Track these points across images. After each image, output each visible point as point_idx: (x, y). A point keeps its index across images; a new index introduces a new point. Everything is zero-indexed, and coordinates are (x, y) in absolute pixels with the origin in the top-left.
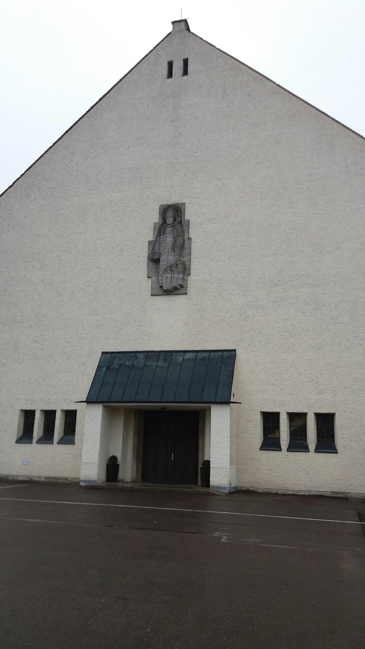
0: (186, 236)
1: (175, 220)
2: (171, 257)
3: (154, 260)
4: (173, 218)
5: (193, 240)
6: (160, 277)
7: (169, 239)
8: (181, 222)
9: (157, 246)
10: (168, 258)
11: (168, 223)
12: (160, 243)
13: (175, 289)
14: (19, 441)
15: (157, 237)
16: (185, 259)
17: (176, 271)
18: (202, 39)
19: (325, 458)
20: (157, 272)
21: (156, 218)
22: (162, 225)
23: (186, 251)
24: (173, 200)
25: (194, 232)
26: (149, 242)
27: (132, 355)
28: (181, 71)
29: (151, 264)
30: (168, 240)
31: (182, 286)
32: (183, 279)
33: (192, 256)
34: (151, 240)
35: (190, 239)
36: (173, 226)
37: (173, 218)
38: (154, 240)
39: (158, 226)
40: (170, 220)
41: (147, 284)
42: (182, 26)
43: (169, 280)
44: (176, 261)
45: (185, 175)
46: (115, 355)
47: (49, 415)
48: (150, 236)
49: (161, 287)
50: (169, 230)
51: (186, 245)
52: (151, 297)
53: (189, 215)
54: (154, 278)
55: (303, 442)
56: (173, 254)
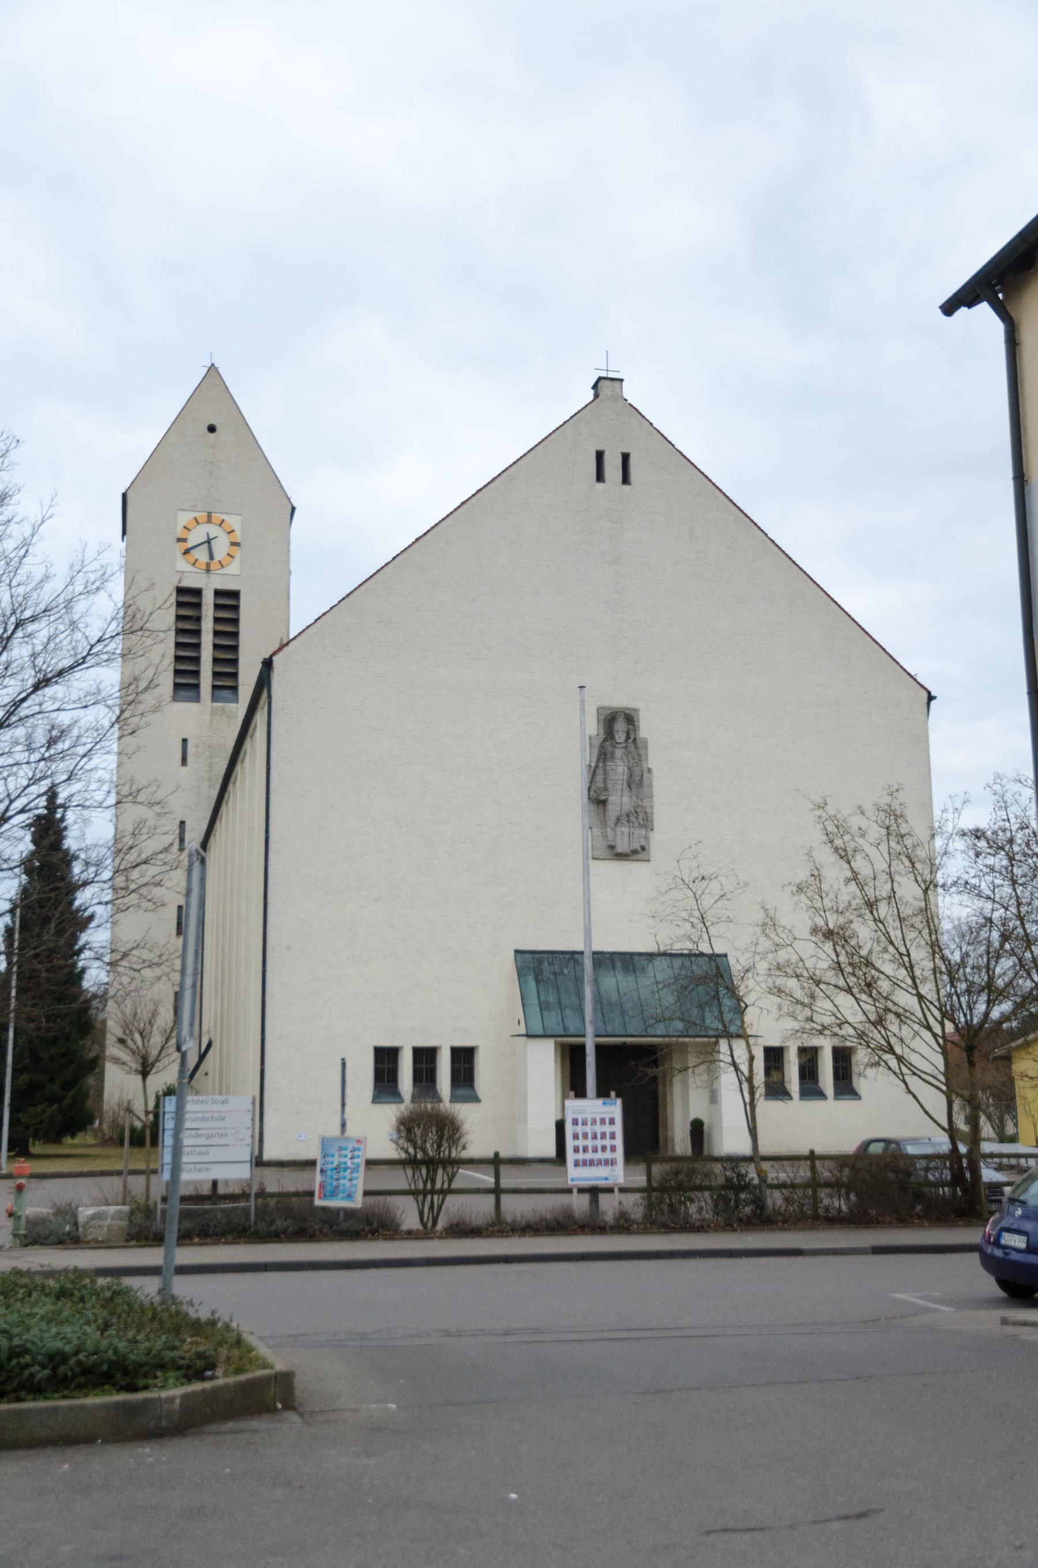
0: (645, 766)
1: (628, 737)
2: (625, 799)
3: (598, 801)
4: (618, 729)
5: (655, 772)
6: (609, 829)
7: (619, 769)
8: (635, 739)
9: (599, 778)
10: (619, 801)
13: (635, 852)
14: (377, 1099)
15: (598, 761)
16: (645, 803)
17: (637, 825)
18: (651, 424)
19: (846, 1106)
20: (603, 822)
21: (593, 727)
22: (605, 740)
24: (619, 701)
25: (655, 759)
27: (567, 956)
28: (607, 457)
29: (593, 807)
30: (620, 769)
31: (643, 848)
32: (647, 838)
33: (655, 799)
35: (649, 770)
36: (626, 748)
37: (618, 729)
38: (593, 765)
39: (597, 743)
40: (620, 737)
43: (626, 838)
46: (538, 956)
47: (425, 1057)
49: (612, 847)
50: (619, 753)
51: (646, 782)
53: (646, 729)
55: (814, 1086)
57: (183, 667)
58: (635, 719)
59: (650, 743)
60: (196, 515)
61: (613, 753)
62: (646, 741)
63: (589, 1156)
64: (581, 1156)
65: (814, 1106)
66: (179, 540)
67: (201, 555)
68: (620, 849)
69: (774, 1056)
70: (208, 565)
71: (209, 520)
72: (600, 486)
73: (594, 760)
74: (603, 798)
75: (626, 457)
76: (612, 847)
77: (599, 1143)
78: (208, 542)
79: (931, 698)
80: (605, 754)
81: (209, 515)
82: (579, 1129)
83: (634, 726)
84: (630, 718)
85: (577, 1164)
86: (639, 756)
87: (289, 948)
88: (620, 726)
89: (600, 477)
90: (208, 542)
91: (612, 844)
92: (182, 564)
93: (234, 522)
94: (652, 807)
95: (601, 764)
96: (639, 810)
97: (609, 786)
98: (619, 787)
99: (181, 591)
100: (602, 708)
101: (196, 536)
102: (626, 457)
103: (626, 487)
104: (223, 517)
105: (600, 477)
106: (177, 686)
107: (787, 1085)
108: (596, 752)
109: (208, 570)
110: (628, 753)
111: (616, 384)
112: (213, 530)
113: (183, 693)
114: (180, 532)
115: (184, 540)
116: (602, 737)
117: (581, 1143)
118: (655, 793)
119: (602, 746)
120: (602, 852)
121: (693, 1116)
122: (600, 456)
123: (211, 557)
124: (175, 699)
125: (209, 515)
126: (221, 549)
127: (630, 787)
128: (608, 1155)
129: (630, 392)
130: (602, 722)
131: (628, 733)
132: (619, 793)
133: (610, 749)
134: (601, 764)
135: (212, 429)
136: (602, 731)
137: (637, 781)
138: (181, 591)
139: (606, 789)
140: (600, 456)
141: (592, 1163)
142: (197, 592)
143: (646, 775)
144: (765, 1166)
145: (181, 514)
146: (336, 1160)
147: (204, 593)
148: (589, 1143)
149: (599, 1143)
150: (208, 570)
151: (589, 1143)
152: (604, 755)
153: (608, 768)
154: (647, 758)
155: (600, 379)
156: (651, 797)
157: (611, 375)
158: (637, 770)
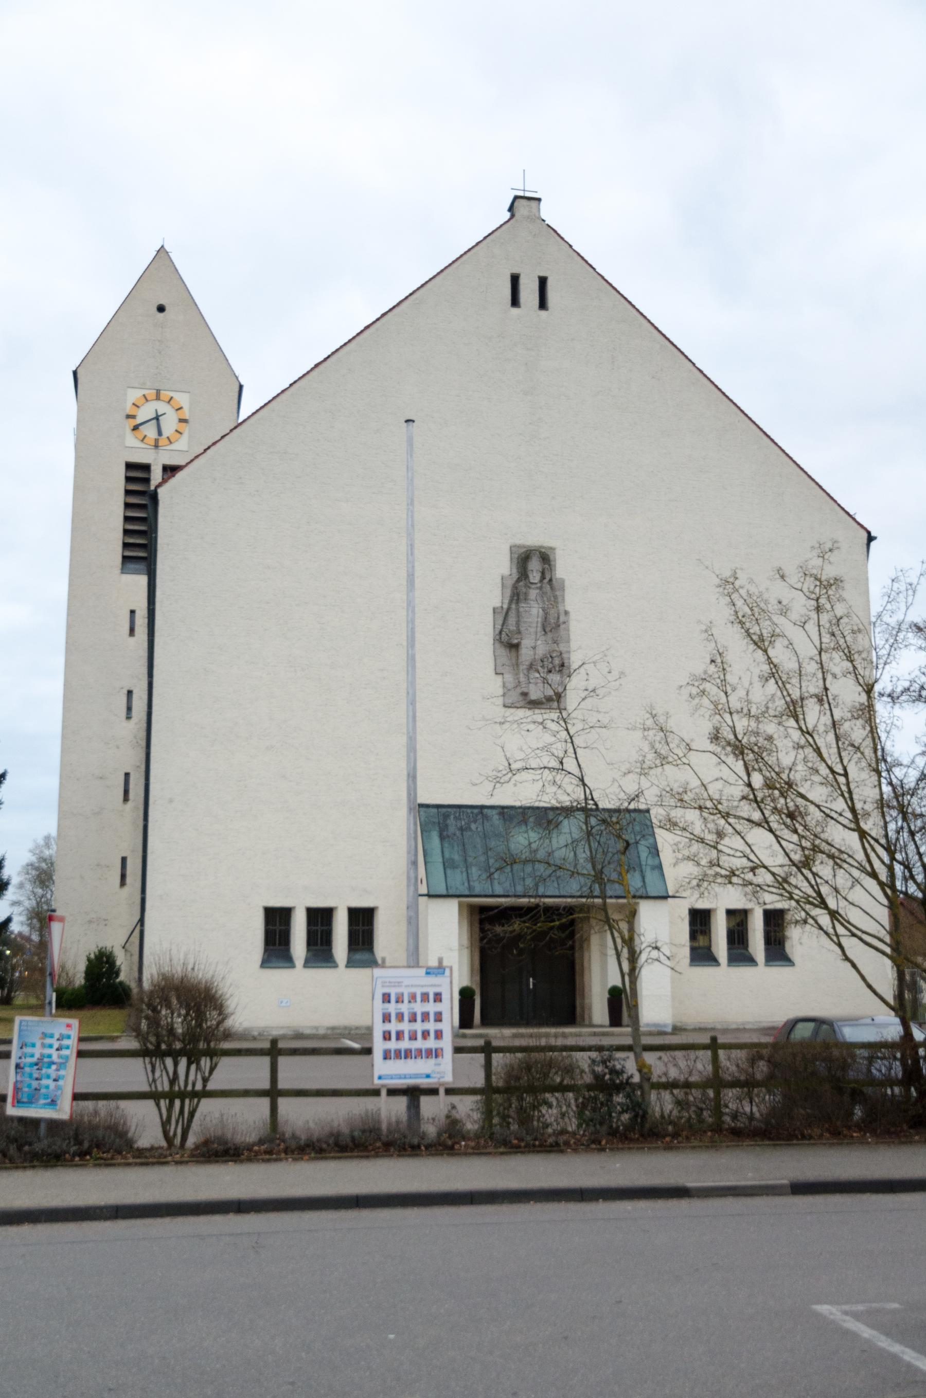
0: (561, 608)
3: (508, 643)
4: (532, 570)
5: (573, 616)
7: (533, 611)
8: (551, 580)
9: (512, 620)
10: (533, 645)
11: (532, 581)
12: (518, 615)
13: (549, 699)
14: (266, 963)
16: (562, 647)
18: (571, 246)
19: (778, 972)
20: (516, 665)
21: (504, 567)
22: (519, 580)
23: (562, 631)
24: (534, 539)
25: (572, 601)
26: (494, 609)
27: (476, 811)
29: (503, 652)
30: (534, 611)
34: (499, 605)
35: (566, 613)
36: (541, 588)
37: (532, 570)
38: (505, 606)
39: (510, 583)
40: (535, 577)
41: (495, 685)
42: (522, 205)
44: (550, 652)
45: (553, 498)
46: (444, 810)
47: (320, 919)
48: (496, 597)
49: (525, 694)
50: (533, 593)
52: (504, 709)
53: (562, 569)
54: (509, 677)
55: (743, 951)
56: (543, 638)
57: (131, 541)
58: (552, 558)
59: (567, 583)
60: (146, 392)
61: (526, 594)
62: (563, 581)
63: (405, 1044)
64: (393, 1045)
65: (744, 972)
66: (129, 417)
67: (150, 431)
68: (533, 696)
69: (700, 920)
70: (157, 441)
71: (158, 398)
72: (515, 311)
73: (507, 601)
74: (516, 641)
75: (543, 282)
76: (525, 694)
77: (419, 1027)
78: (157, 418)
79: (870, 538)
80: (518, 595)
81: (158, 392)
82: (392, 1008)
83: (550, 565)
84: (546, 558)
85: (387, 1055)
86: (556, 597)
87: (171, 801)
88: (535, 565)
89: (515, 302)
90: (157, 418)
91: (525, 690)
92: (131, 440)
93: (182, 399)
94: (569, 652)
95: (513, 606)
96: (554, 655)
97: (522, 629)
98: (532, 630)
99: (130, 466)
100: (515, 546)
101: (146, 412)
102: (543, 282)
103: (543, 313)
104: (171, 394)
105: (515, 302)
106: (125, 559)
107: (714, 949)
108: (508, 593)
109: (156, 446)
110: (543, 594)
111: (534, 204)
112: (162, 407)
113: (131, 566)
114: (129, 409)
115: (133, 417)
117: (393, 1027)
118: (572, 637)
120: (514, 696)
122: (515, 280)
123: (160, 433)
124: (124, 570)
125: (158, 392)
126: (169, 425)
127: (544, 631)
128: (431, 1043)
129: (547, 212)
130: (515, 561)
131: (543, 573)
132: (533, 637)
133: (524, 590)
134: (513, 606)
135: (161, 309)
136: (515, 571)
137: (554, 625)
138: (130, 466)
139: (519, 632)
140: (515, 280)
141: (408, 1054)
142: (146, 468)
143: (562, 619)
144: (650, 1058)
145: (130, 390)
146: (37, 1052)
147: (152, 468)
148: (405, 1026)
149: (419, 1027)
150: (156, 446)
151: (405, 1026)
152: (517, 596)
153: (521, 610)
154: (563, 600)
155: (516, 198)
156: (568, 641)
157: (528, 194)
158: (552, 612)
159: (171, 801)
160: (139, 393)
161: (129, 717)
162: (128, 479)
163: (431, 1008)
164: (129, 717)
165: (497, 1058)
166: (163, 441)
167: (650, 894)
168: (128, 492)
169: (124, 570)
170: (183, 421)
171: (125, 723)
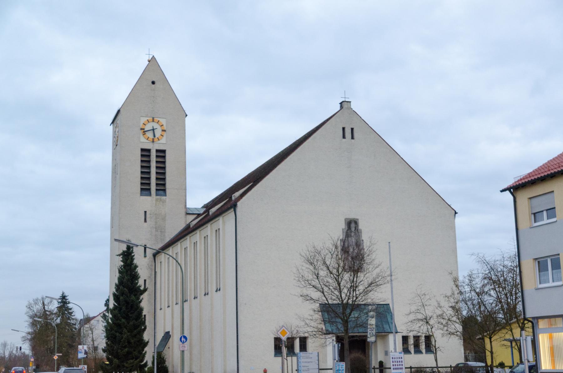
1: (355, 229)
22: (348, 230)
24: (352, 216)
39: (345, 231)
40: (353, 229)
53: (361, 226)
57: (144, 182)
60: (148, 118)
63: (396, 367)
64: (394, 367)
65: (419, 356)
66: (141, 129)
67: (150, 135)
69: (405, 339)
70: (153, 139)
71: (153, 121)
72: (344, 140)
75: (352, 129)
77: (399, 363)
78: (153, 130)
79: (456, 213)
81: (153, 119)
82: (394, 360)
84: (356, 222)
85: (393, 369)
87: (246, 304)
88: (353, 225)
89: (344, 137)
90: (153, 130)
92: (143, 139)
93: (163, 121)
99: (142, 150)
101: (148, 127)
102: (352, 129)
103: (353, 140)
104: (158, 119)
105: (344, 137)
106: (141, 189)
107: (409, 349)
108: (345, 234)
109: (153, 142)
111: (349, 103)
112: (156, 126)
113: (144, 192)
114: (141, 126)
115: (144, 129)
116: (347, 229)
117: (394, 364)
119: (347, 233)
121: (379, 360)
122: (344, 129)
123: (154, 136)
124: (141, 195)
125: (153, 119)
126: (158, 133)
128: (401, 367)
129: (353, 106)
135: (153, 83)
138: (142, 150)
140: (344, 129)
141: (397, 369)
142: (149, 151)
144: (439, 369)
145: (142, 118)
146: (337, 368)
147: (152, 151)
148: (396, 363)
149: (399, 363)
150: (153, 142)
151: (396, 363)
155: (343, 102)
157: (347, 100)
159: (246, 304)
160: (146, 119)
161: (145, 256)
162: (142, 156)
163: (400, 360)
164: (145, 256)
165: (413, 370)
166: (156, 139)
167: (493, 343)
168: (142, 161)
169: (141, 195)
170: (164, 131)
171: (144, 259)
